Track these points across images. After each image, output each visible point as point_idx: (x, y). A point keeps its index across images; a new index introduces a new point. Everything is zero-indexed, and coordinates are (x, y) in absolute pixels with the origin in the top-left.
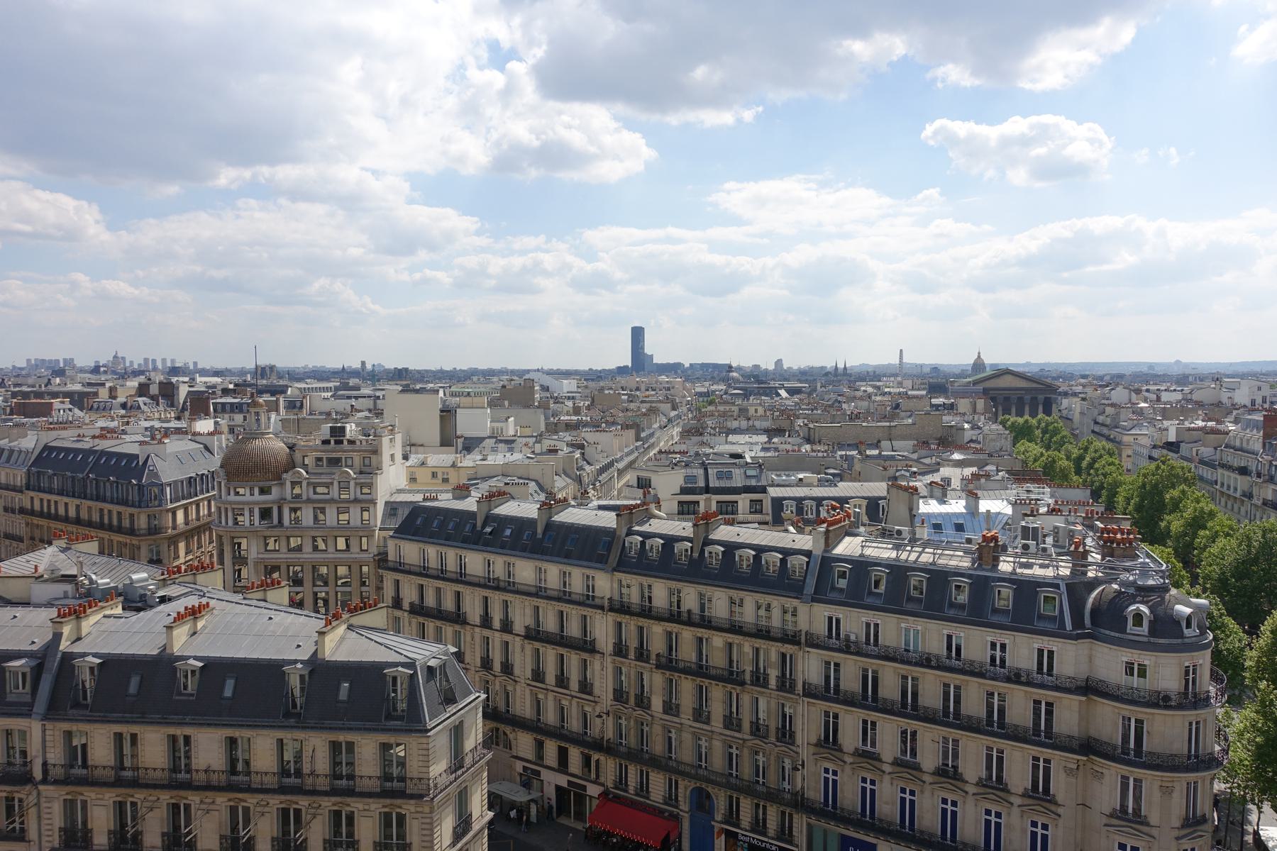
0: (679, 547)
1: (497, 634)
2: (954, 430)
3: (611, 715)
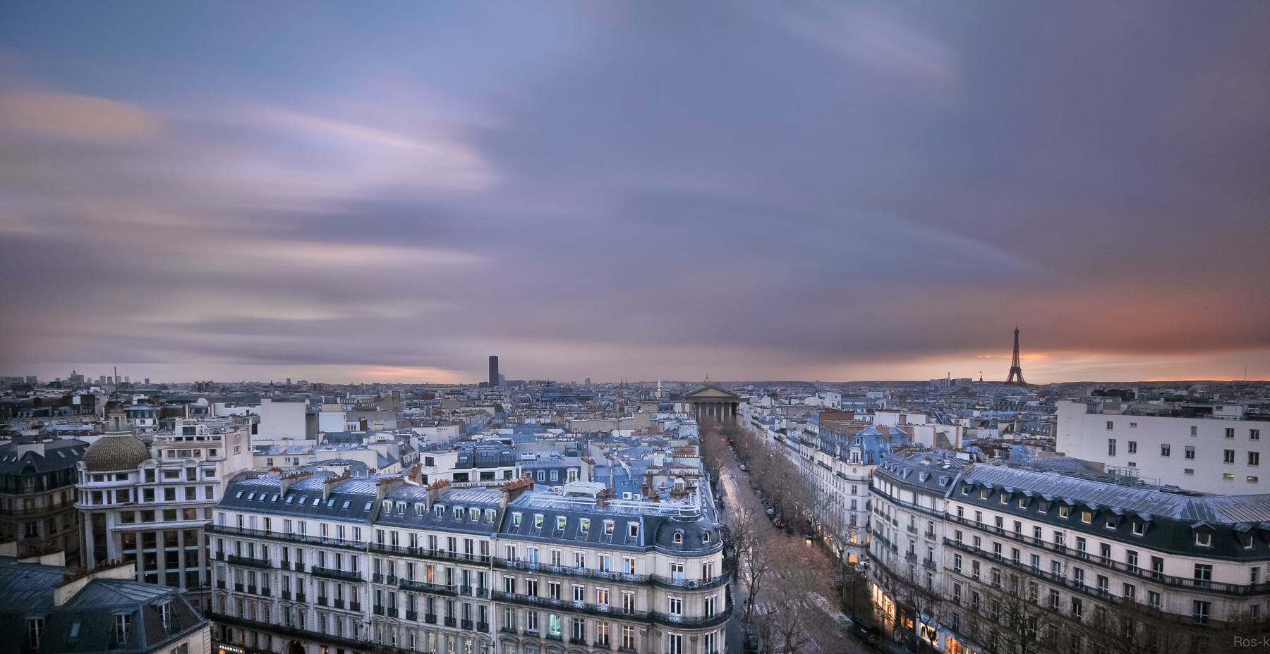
0: (417, 505)
1: (293, 574)
3: (372, 624)
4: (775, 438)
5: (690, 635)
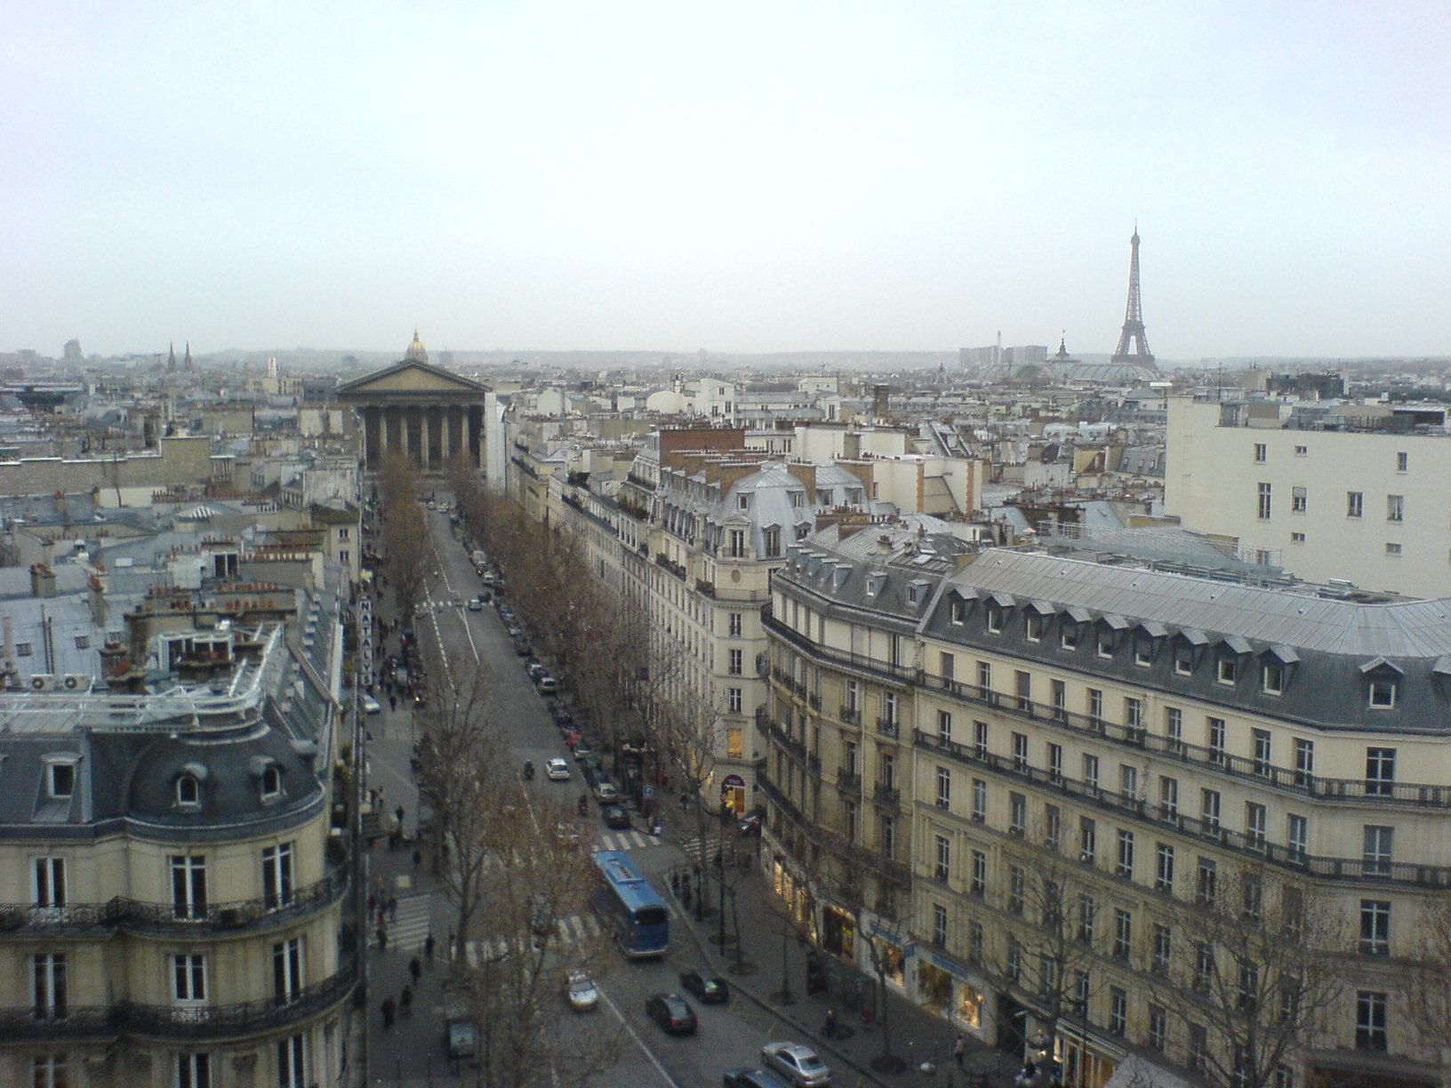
2: (231, 467)
4: (565, 498)
5: (232, 1055)
